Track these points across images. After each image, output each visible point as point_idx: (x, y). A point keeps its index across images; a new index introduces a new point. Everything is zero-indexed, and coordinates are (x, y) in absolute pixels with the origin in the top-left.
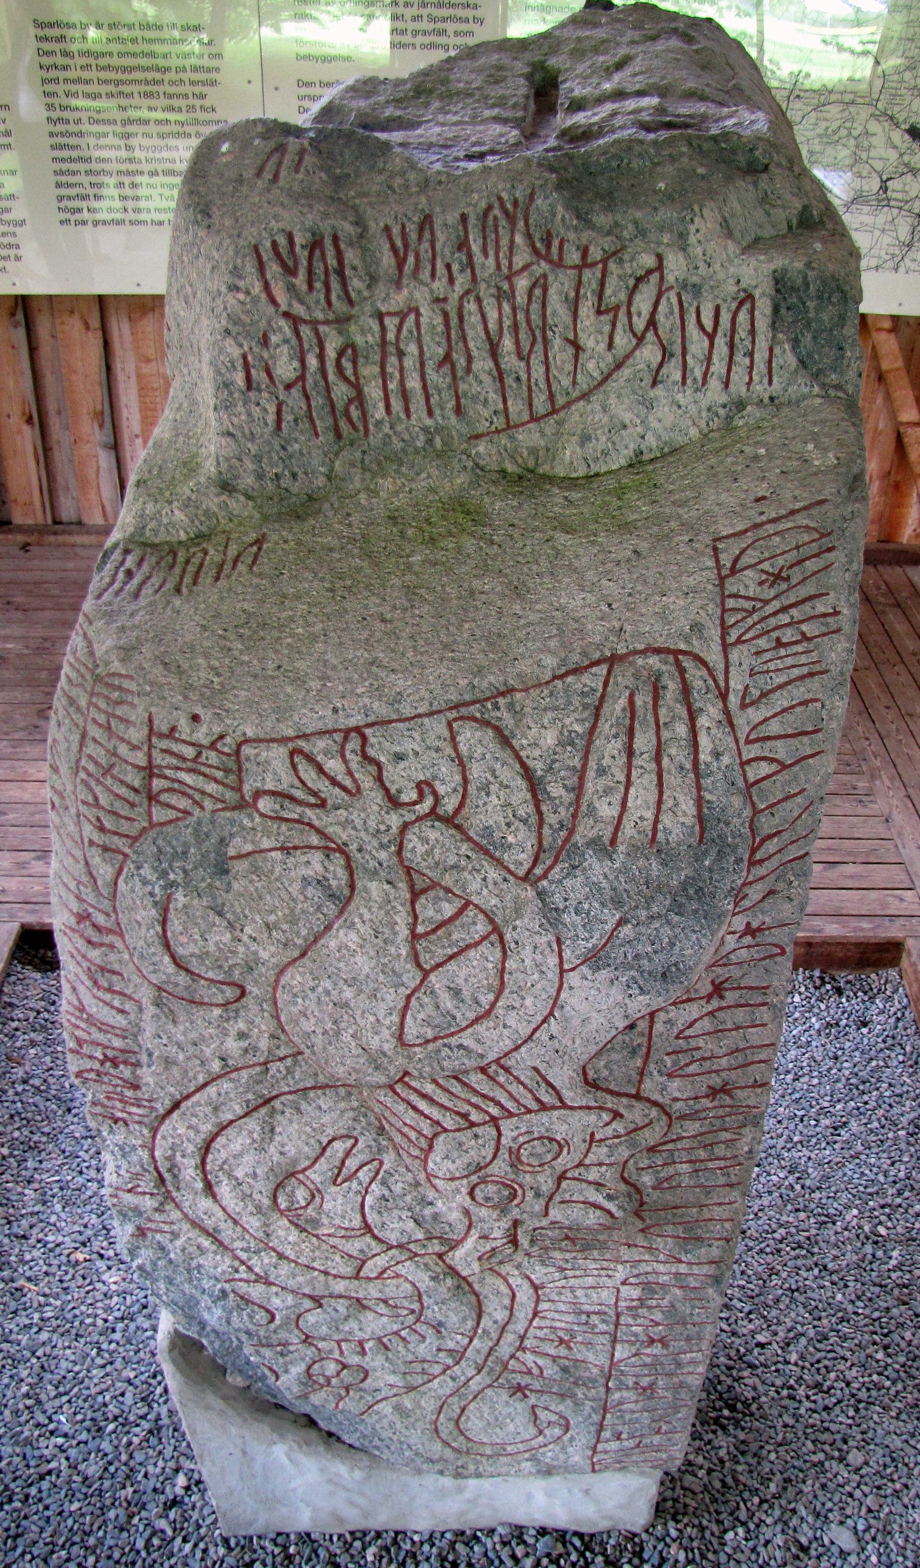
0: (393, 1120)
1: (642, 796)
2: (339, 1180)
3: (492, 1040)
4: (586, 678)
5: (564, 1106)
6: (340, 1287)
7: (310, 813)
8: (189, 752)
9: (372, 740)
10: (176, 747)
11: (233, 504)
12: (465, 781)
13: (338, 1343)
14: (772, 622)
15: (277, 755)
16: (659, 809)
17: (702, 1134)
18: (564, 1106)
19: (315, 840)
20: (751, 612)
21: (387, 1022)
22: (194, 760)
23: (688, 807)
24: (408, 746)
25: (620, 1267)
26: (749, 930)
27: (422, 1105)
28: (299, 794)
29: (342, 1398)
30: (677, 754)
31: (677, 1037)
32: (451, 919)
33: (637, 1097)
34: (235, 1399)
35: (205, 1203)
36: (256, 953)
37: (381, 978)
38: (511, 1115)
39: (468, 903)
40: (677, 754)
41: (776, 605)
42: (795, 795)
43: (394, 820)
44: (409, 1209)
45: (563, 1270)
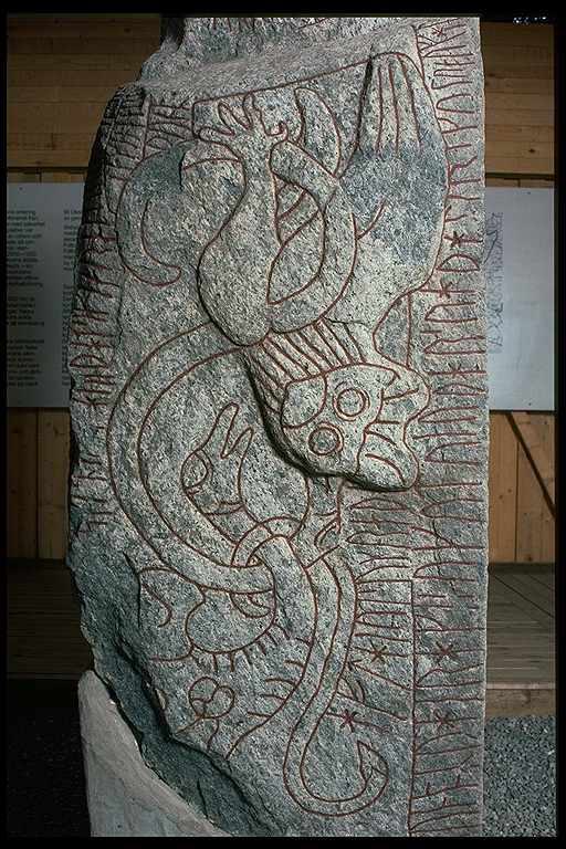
0: (264, 376)
1: (390, 122)
2: (226, 453)
3: (318, 299)
4: (357, 69)
5: (364, 363)
6: (221, 576)
7: (227, 138)
8: (170, 111)
9: (258, 99)
10: (162, 110)
11: (190, 61)
12: (304, 120)
13: (214, 654)
14: (441, 53)
15: (213, 106)
16: (398, 131)
17: (451, 408)
18: (364, 363)
19: (228, 153)
20: (432, 45)
21: (260, 283)
22: (171, 117)
23: (411, 127)
24: (275, 102)
25: (410, 553)
26: (457, 240)
27: (280, 356)
28: (222, 128)
29: (215, 732)
30: (404, 100)
31: (426, 319)
32: (296, 206)
33: (408, 367)
34: (135, 666)
35: (138, 486)
36: (190, 236)
37: (259, 249)
38: (333, 369)
39: (307, 191)
40: (404, 100)
41: (440, 46)
42: (467, 145)
43: (269, 142)
44: (270, 482)
45: (374, 557)
